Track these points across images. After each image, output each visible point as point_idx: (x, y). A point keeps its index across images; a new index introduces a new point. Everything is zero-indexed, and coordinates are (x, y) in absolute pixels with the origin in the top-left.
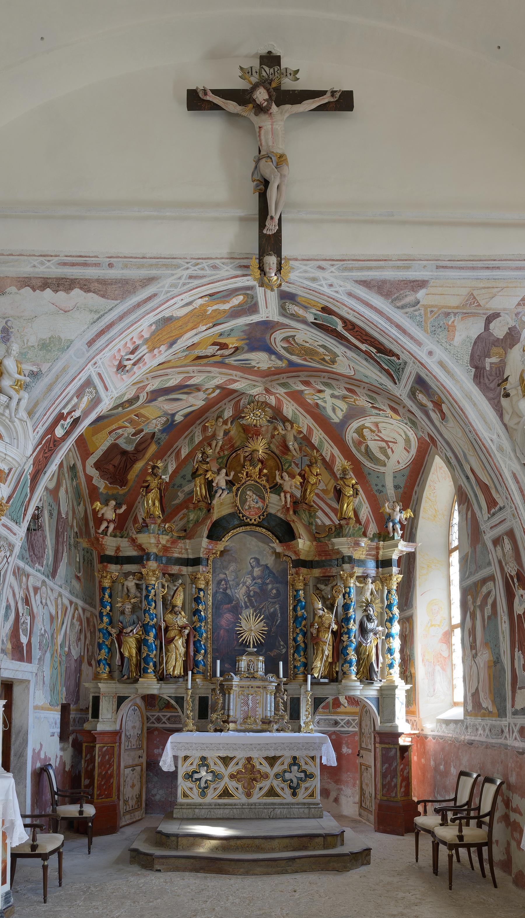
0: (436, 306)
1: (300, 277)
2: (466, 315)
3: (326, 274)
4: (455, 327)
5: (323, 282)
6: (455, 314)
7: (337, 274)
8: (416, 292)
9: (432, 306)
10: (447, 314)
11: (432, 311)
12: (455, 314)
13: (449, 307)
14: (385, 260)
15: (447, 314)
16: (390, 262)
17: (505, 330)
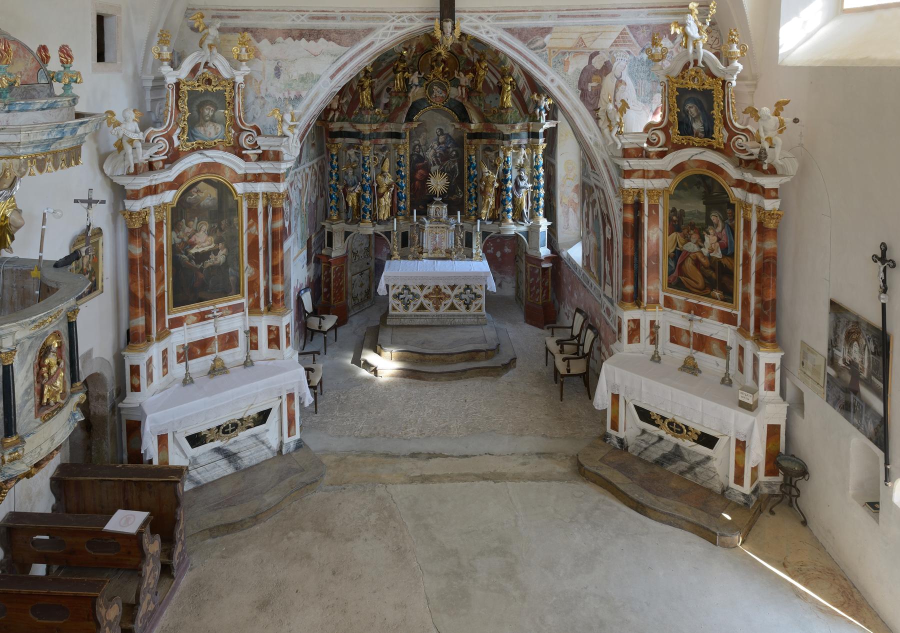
0: (556, 48)
1: (467, 26)
2: (577, 53)
3: (485, 24)
4: (569, 62)
5: (483, 30)
6: (569, 53)
7: (492, 23)
8: (544, 37)
9: (554, 48)
10: (564, 53)
11: (554, 52)
12: (569, 53)
13: (565, 48)
14: (524, 11)
15: (564, 53)
16: (527, 13)
17: (603, 63)
